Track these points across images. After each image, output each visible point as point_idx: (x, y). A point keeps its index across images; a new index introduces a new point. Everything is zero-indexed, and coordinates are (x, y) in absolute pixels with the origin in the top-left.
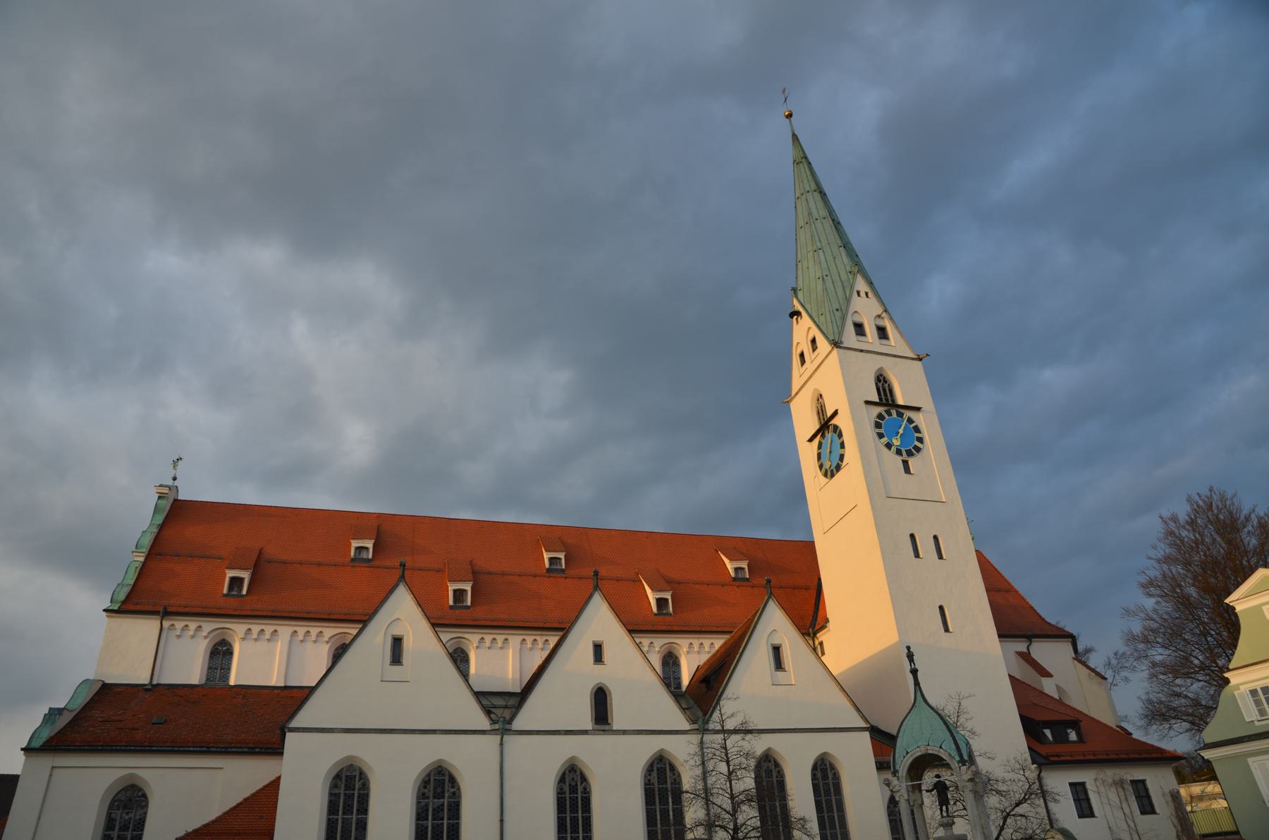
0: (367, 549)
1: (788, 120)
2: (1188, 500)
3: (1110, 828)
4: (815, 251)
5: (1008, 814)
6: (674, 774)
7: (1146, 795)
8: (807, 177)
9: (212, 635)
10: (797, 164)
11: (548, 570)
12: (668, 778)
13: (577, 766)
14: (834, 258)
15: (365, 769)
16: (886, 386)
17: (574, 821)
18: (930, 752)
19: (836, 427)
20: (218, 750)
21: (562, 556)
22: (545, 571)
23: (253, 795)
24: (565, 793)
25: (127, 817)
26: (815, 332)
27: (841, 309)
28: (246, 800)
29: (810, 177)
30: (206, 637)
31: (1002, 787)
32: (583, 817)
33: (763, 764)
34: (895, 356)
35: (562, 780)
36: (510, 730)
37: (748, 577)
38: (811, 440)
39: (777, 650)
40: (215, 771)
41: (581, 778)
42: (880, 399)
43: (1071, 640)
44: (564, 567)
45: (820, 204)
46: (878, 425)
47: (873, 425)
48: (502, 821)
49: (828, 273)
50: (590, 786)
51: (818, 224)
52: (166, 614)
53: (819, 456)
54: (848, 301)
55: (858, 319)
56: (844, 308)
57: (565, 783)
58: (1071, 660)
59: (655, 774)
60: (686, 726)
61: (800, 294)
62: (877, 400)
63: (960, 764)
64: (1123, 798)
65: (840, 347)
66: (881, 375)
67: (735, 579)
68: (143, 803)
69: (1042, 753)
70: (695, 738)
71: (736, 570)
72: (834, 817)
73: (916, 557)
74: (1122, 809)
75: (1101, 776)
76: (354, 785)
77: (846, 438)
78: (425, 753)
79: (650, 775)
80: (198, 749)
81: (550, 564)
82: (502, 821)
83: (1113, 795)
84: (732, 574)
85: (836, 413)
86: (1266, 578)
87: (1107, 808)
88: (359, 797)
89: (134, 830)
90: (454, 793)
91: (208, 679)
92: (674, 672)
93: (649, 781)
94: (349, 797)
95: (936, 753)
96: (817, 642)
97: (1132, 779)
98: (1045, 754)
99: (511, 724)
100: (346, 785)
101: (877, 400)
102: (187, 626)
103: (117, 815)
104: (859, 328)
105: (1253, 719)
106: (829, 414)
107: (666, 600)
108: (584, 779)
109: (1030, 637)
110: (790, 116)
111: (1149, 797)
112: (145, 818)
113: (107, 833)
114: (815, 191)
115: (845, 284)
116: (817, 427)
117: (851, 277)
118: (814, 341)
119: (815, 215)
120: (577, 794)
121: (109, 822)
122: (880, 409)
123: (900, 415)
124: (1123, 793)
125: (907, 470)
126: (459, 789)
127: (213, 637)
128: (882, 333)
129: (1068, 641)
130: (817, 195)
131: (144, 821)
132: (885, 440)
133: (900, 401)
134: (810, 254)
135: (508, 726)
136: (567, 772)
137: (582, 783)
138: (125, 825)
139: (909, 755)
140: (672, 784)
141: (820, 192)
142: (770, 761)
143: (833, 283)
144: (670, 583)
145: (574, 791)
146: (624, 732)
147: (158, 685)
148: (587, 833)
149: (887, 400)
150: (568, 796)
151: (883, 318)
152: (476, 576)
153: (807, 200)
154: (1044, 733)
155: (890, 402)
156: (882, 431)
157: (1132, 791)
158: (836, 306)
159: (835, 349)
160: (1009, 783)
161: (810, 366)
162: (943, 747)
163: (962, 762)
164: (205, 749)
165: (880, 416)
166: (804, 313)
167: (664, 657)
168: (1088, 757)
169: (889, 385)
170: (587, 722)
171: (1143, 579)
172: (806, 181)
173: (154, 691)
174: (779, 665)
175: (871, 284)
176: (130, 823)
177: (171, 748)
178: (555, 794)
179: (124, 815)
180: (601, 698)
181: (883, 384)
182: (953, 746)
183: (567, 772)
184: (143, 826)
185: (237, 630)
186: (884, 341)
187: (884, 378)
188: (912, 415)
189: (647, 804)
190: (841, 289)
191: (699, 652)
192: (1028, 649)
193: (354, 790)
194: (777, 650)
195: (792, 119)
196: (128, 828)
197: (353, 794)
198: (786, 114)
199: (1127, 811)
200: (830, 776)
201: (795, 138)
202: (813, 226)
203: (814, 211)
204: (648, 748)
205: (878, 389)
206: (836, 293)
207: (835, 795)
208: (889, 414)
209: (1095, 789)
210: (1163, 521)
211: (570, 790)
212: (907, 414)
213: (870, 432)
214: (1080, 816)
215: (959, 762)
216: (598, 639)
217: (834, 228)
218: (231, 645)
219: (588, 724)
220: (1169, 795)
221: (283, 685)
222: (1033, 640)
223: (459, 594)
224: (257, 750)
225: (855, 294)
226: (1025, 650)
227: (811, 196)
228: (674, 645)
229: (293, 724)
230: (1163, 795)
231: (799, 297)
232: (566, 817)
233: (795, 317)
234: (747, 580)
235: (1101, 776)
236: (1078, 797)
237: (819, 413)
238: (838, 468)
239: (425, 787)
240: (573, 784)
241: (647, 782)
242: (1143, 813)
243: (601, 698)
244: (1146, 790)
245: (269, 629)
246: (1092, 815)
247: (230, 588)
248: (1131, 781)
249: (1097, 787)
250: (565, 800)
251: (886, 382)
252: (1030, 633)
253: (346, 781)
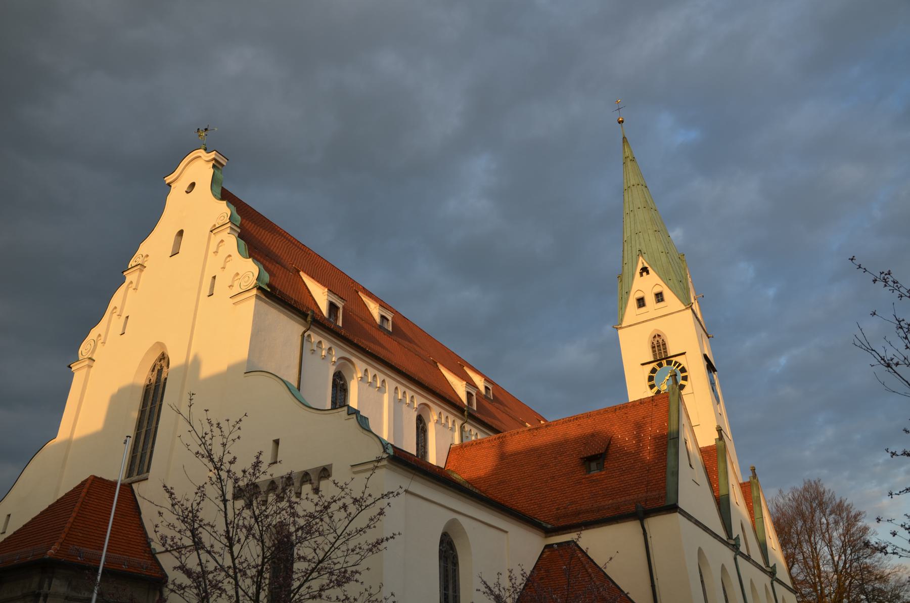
4: (656, 231)
53: (651, 379)
56: (684, 281)
61: (643, 255)
85: (684, 354)
134: (650, 232)
159: (690, 310)
198: (620, 119)
218: (345, 382)
237: (653, 347)
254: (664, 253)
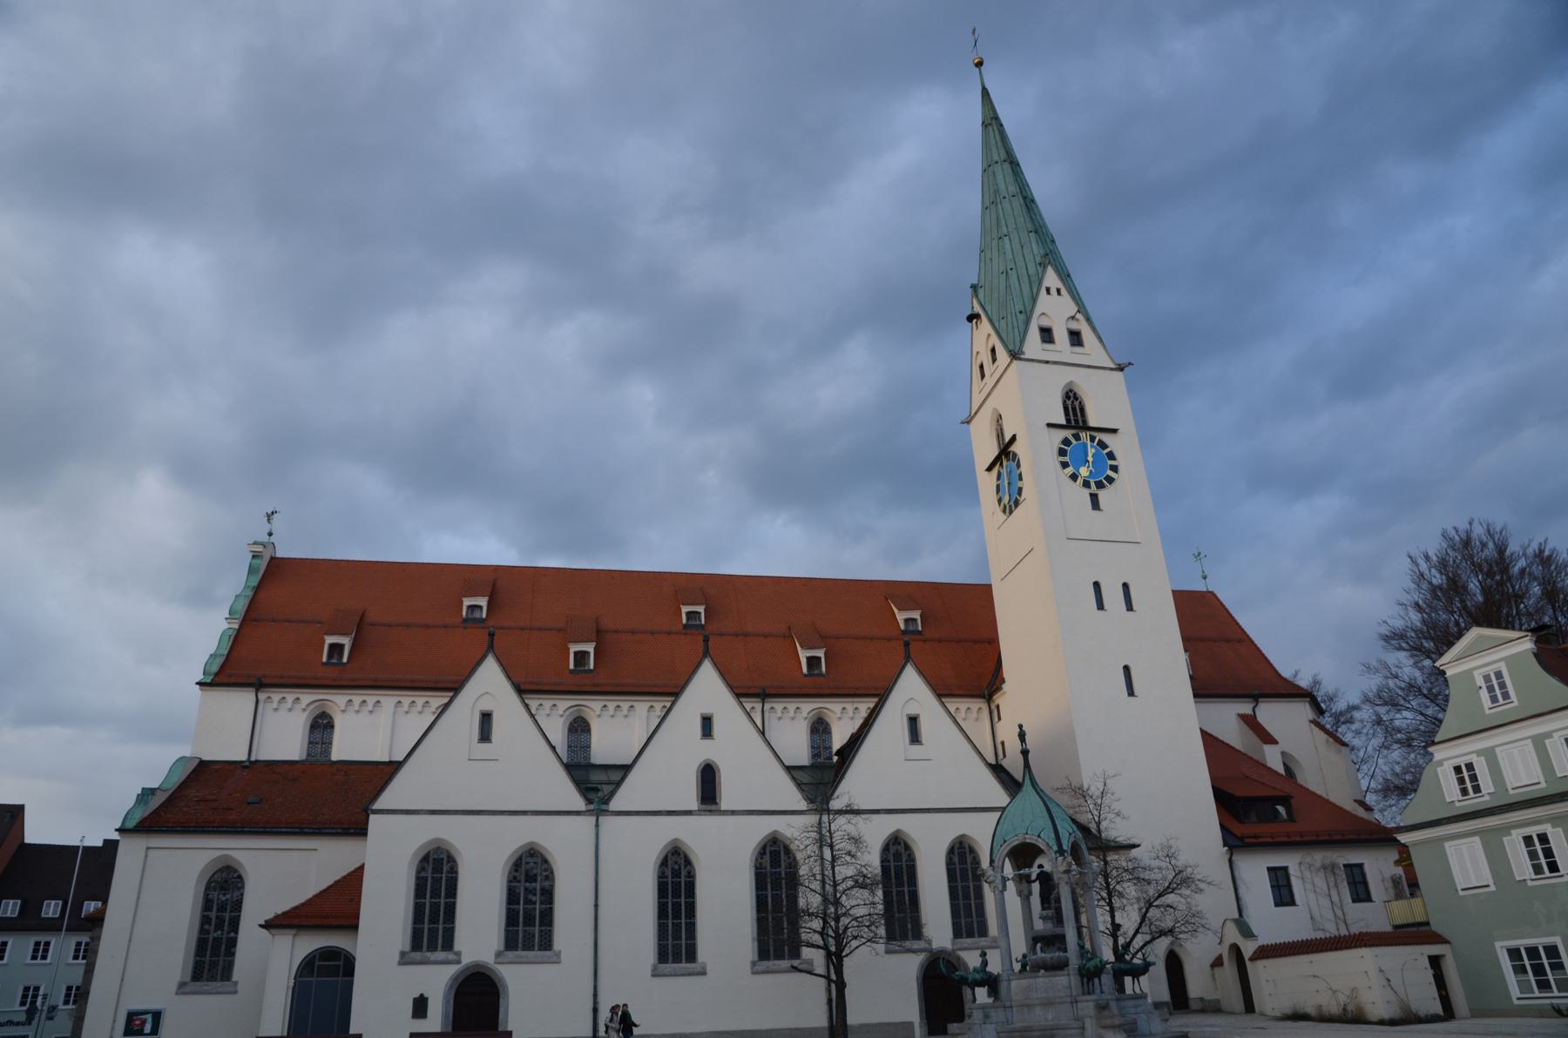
0: (480, 607)
1: (977, 69)
2: (1443, 536)
3: (1312, 918)
5: (1151, 905)
6: (789, 858)
7: (1362, 880)
8: (996, 143)
9: (312, 707)
10: (986, 126)
11: (685, 626)
12: (782, 862)
13: (680, 848)
14: (1022, 247)
15: (453, 852)
16: (1077, 403)
17: (677, 906)
18: (1028, 841)
19: (1015, 455)
20: (311, 831)
21: (701, 609)
22: (681, 627)
23: (344, 877)
24: (667, 877)
25: (224, 899)
26: (995, 340)
27: (1026, 312)
28: (337, 883)
29: (1000, 144)
30: (304, 710)
31: (1146, 875)
32: (686, 903)
33: (891, 846)
34: (1089, 367)
35: (664, 863)
36: (608, 811)
37: (920, 629)
38: (989, 469)
39: (913, 721)
40: (308, 853)
41: (685, 861)
42: (1068, 420)
43: (1308, 699)
44: (703, 622)
45: (1010, 178)
46: (1062, 452)
47: (1056, 451)
48: (596, 906)
49: (1013, 266)
50: (694, 870)
51: (1006, 205)
52: (259, 685)
54: (1034, 300)
55: (1045, 323)
56: (1028, 309)
57: (667, 866)
58: (1308, 723)
59: (767, 857)
60: (803, 805)
61: (981, 292)
62: (1064, 422)
63: (1058, 855)
64: (1332, 884)
65: (1020, 359)
66: (1071, 391)
67: (904, 632)
68: (239, 885)
69: (1236, 833)
70: (812, 819)
71: (907, 621)
72: (970, 905)
73: (1098, 609)
74: (1330, 896)
75: (1307, 860)
76: (442, 869)
77: (1023, 469)
78: (515, 836)
79: (762, 858)
80: (292, 830)
81: (688, 619)
82: (596, 906)
83: (1320, 881)
84: (902, 626)
85: (1014, 438)
86: (1481, 637)
87: (1312, 896)
88: (447, 880)
89: (232, 912)
90: (547, 878)
91: (309, 755)
92: (824, 741)
93: (761, 864)
94: (437, 881)
95: (1034, 842)
96: (993, 706)
97: (1346, 862)
98: (1239, 835)
99: (608, 804)
100: (433, 869)
101: (1064, 422)
102: (284, 698)
103: (214, 895)
104: (1047, 335)
105: (1453, 799)
106: (1007, 439)
107: (819, 659)
108: (688, 862)
109: (1256, 698)
110: (979, 64)
111: (1365, 883)
112: (242, 899)
113: (205, 913)
114: (1005, 161)
115: (1034, 279)
116: (996, 452)
117: (1040, 270)
118: (993, 350)
119: (1003, 192)
120: (680, 878)
121: (206, 903)
122: (1068, 433)
123: (1092, 439)
124: (1332, 879)
125: (1095, 502)
126: (552, 872)
127: (311, 711)
128: (1075, 338)
129: (1305, 702)
130: (1007, 166)
131: (241, 903)
132: (1070, 470)
133: (1092, 423)
134: (995, 242)
135: (604, 807)
136: (669, 855)
137: (686, 866)
138: (222, 907)
139: (1006, 844)
140: (786, 868)
141: (1011, 163)
142: (899, 844)
143: (1018, 278)
144: (823, 639)
145: (676, 876)
146: (733, 813)
147: (257, 761)
148: (690, 919)
149: (1076, 421)
150: (670, 880)
151: (1077, 320)
152: (599, 636)
153: (994, 173)
154: (1277, 810)
155: (1081, 424)
156: (1066, 459)
157: (1344, 876)
158: (1019, 307)
160: (1156, 871)
161: (990, 381)
162: (1041, 835)
163: (1061, 852)
164: (297, 830)
165: (1066, 442)
166: (983, 316)
167: (813, 724)
168: (1294, 839)
169: (1080, 403)
170: (691, 801)
171: (1384, 630)
172: (994, 150)
173: (252, 767)
174: (915, 737)
175: (1065, 276)
176: (227, 904)
177: (262, 830)
178: (656, 878)
179: (221, 896)
180: (708, 778)
181: (1073, 402)
182: (1053, 835)
183: (669, 855)
184: (241, 907)
185: (337, 701)
186: (1078, 349)
187: (1075, 394)
188: (1105, 437)
189: (757, 889)
190: (1028, 285)
191: (852, 718)
192: (1254, 711)
193: (442, 873)
194: (913, 721)
195: (982, 68)
196: (226, 909)
197: (441, 878)
198: (976, 61)
199: (1335, 898)
200: (969, 860)
201: (985, 92)
202: (1000, 206)
203: (1002, 186)
204: (762, 828)
206: (1021, 289)
207: (973, 881)
208: (1077, 437)
209: (1299, 874)
210: (1412, 561)
211: (672, 873)
212: (1099, 436)
213: (1053, 460)
214: (1277, 905)
215: (1056, 852)
216: (707, 711)
217: (1024, 208)
218: (331, 718)
219: (694, 804)
220: (1390, 881)
221: (387, 760)
222: (1260, 700)
223: (581, 657)
224: (352, 831)
225: (1043, 291)
226: (1250, 712)
227: (1000, 168)
228: (825, 711)
229: (377, 806)
230: (1383, 881)
231: (979, 296)
232: (667, 902)
233: (975, 321)
234: (920, 633)
235: (1308, 860)
236: (1278, 883)
237: (998, 437)
238: (1017, 503)
239: (516, 871)
240: (676, 867)
241: (758, 865)
242: (1354, 901)
243: (708, 778)
244: (1363, 875)
245: (371, 700)
246: (1292, 903)
247: (330, 656)
248: (1345, 866)
249: (1302, 872)
250: (667, 885)
251: (1077, 399)
252: (1256, 692)
253: (434, 864)
254: (1005, 273)
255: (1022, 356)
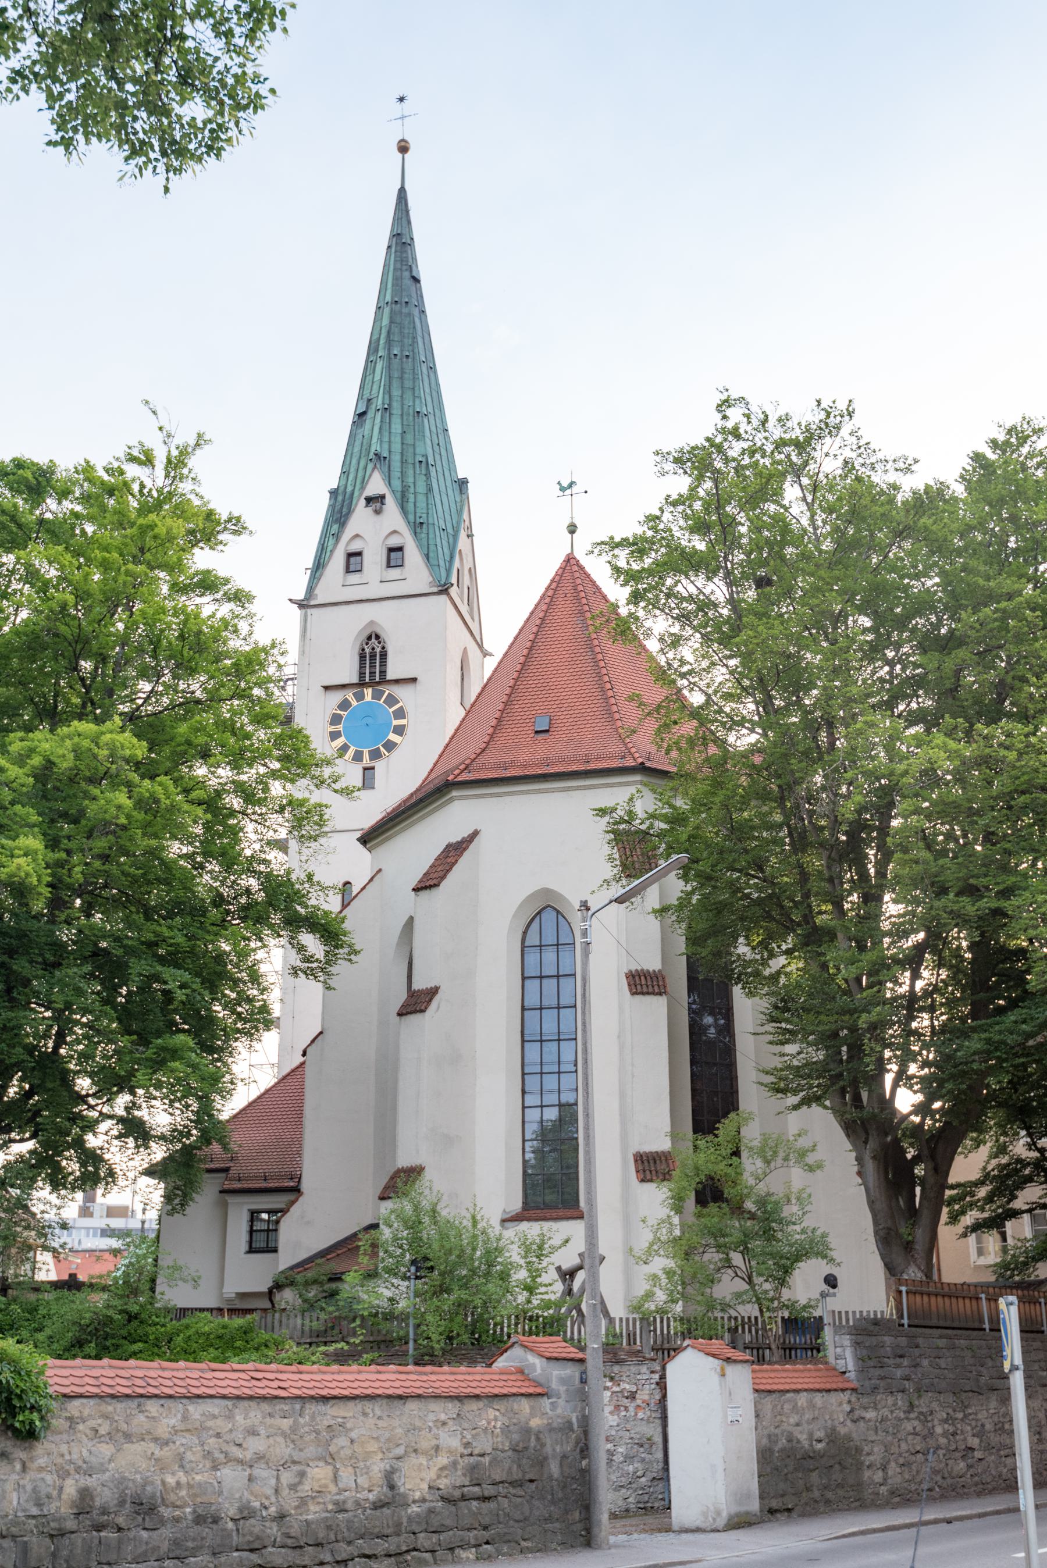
42: (362, 675)
46: (336, 720)
55: (355, 547)
110: (403, 148)
165: (344, 705)
188: (398, 691)
201: (402, 195)
205: (362, 657)
208: (360, 697)
255: (312, 603)
